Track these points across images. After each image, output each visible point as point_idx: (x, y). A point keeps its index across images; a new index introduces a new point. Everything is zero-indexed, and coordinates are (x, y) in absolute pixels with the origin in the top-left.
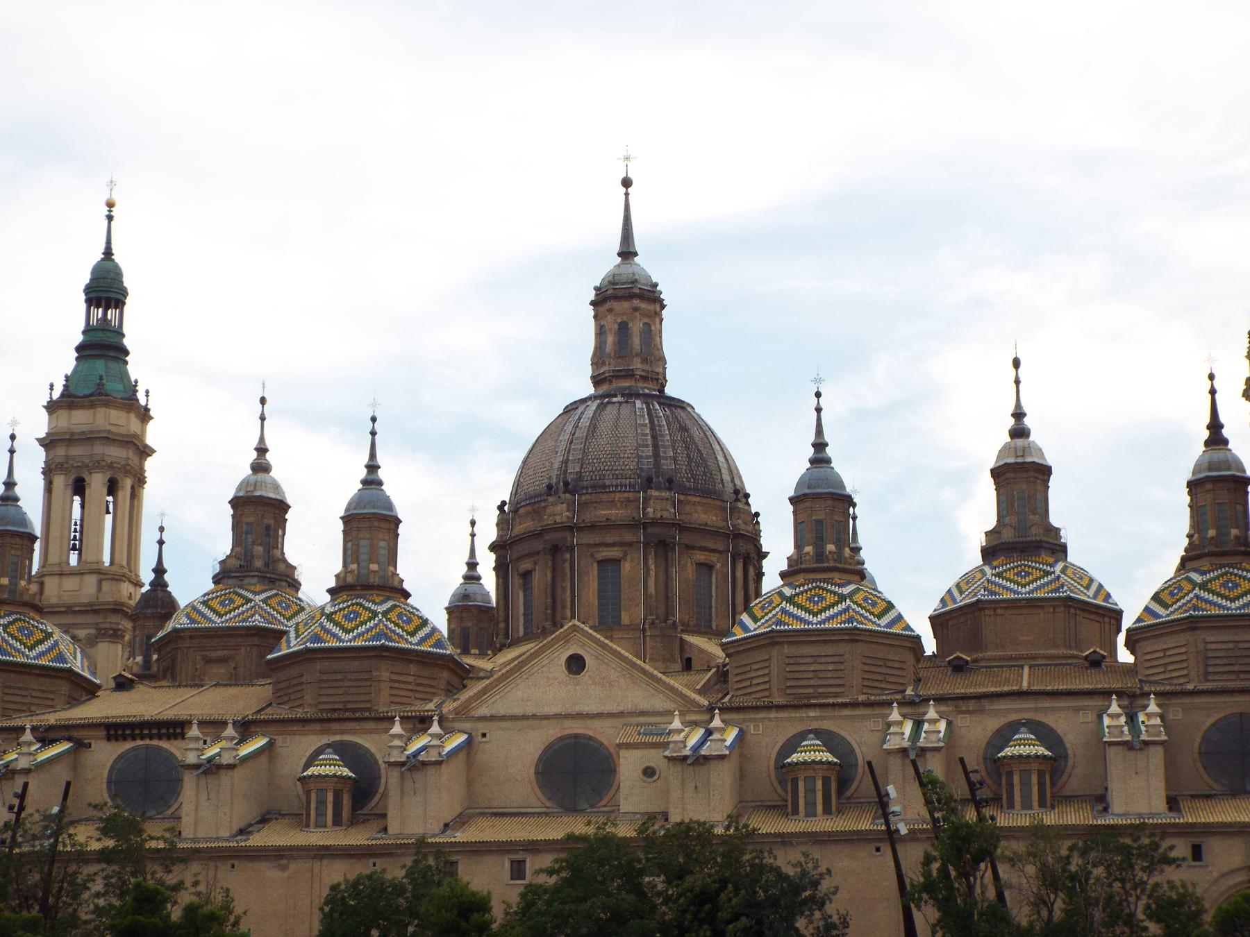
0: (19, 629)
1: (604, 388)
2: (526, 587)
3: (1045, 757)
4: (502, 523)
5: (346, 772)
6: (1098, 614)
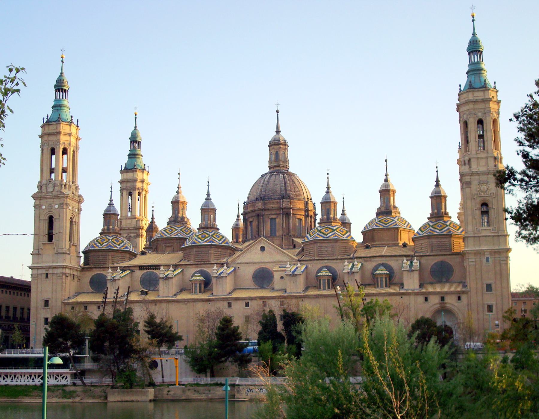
0: (116, 240)
1: (272, 170)
2: (251, 225)
3: (387, 274)
4: (245, 207)
5: (202, 278)
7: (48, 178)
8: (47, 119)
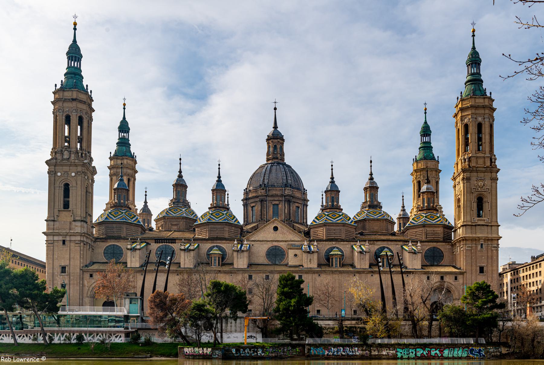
1: (270, 162)
5: (220, 252)
6: (391, 223)
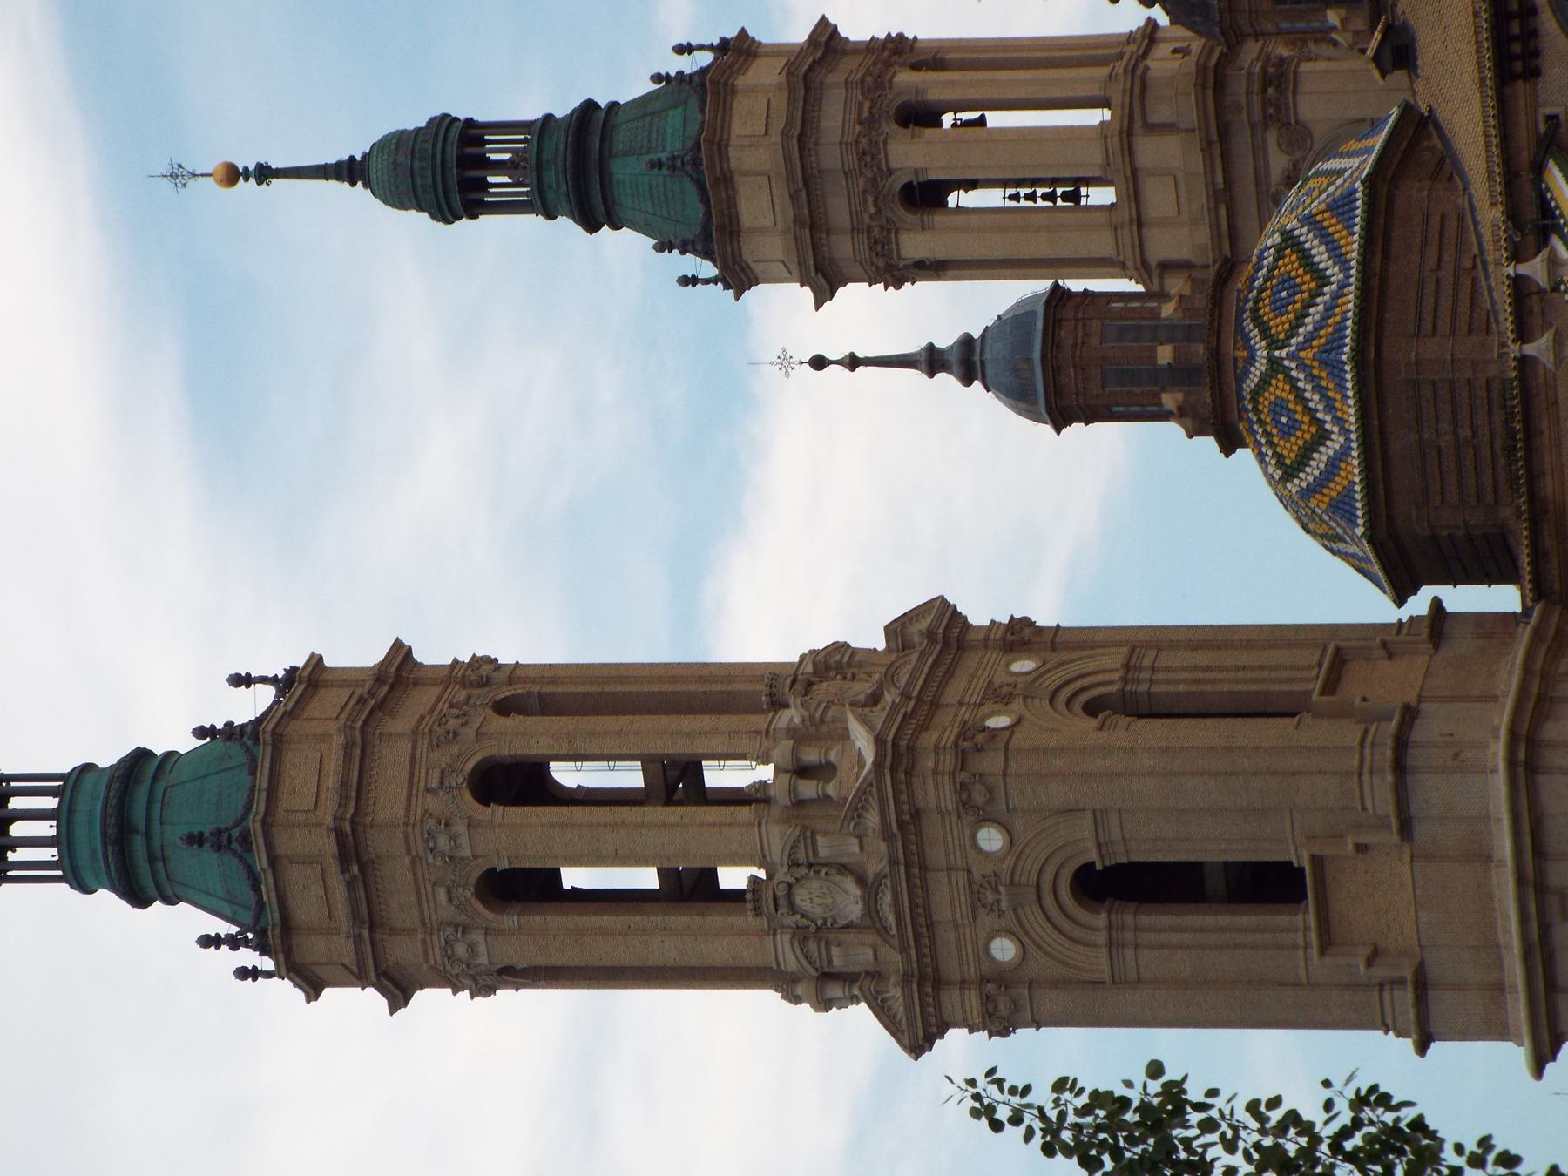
0: (1279, 309)
7: (744, 919)
8: (234, 943)
